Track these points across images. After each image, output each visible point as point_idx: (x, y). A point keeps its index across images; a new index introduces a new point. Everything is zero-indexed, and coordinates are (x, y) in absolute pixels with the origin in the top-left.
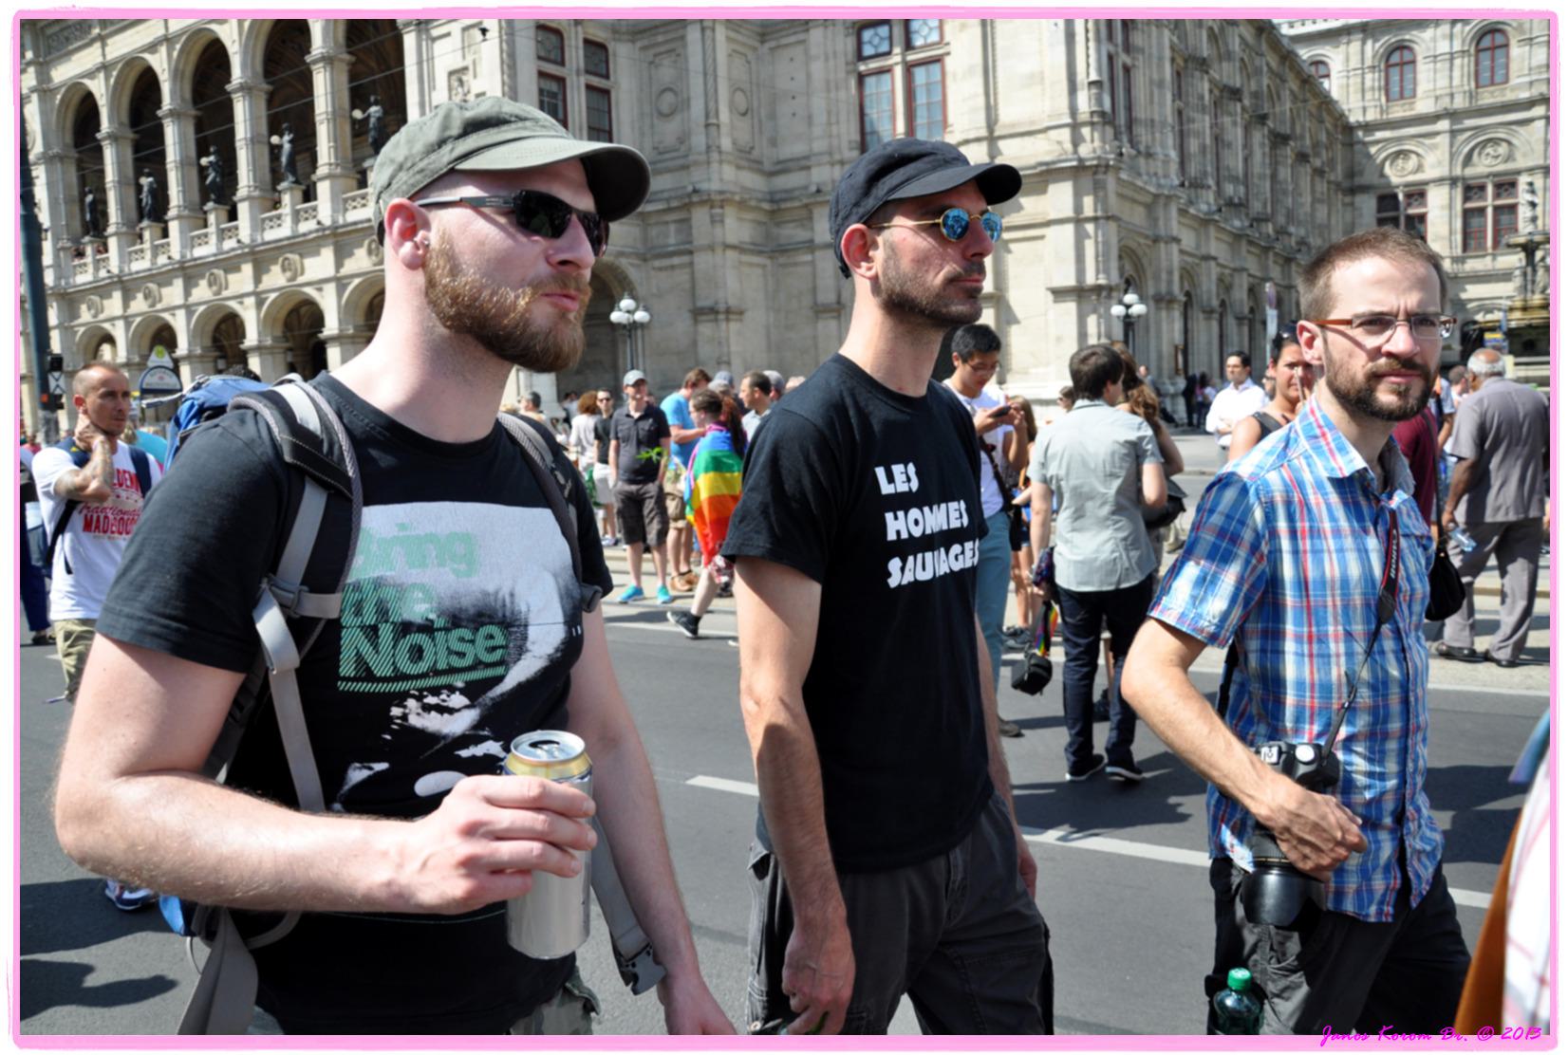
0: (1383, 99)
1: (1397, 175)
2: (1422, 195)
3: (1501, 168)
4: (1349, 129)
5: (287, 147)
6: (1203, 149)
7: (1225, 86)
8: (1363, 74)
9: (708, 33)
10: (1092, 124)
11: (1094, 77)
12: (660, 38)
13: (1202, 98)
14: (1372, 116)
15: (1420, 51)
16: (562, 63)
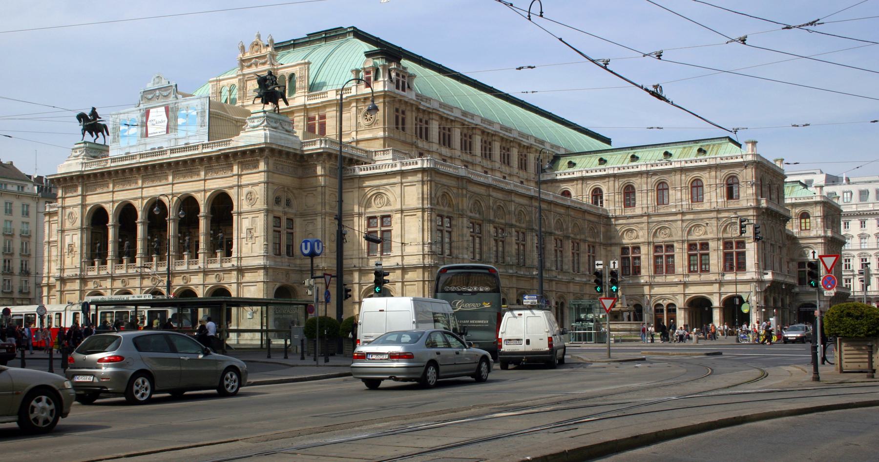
0: (623, 206)
1: (627, 240)
2: (639, 248)
3: (667, 239)
4: (608, 218)
5: (187, 240)
6: (489, 249)
7: (506, 224)
8: (614, 195)
9: (323, 219)
10: (428, 254)
11: (429, 241)
12: (309, 218)
13: (490, 232)
14: (618, 213)
15: (636, 186)
16: (280, 227)
